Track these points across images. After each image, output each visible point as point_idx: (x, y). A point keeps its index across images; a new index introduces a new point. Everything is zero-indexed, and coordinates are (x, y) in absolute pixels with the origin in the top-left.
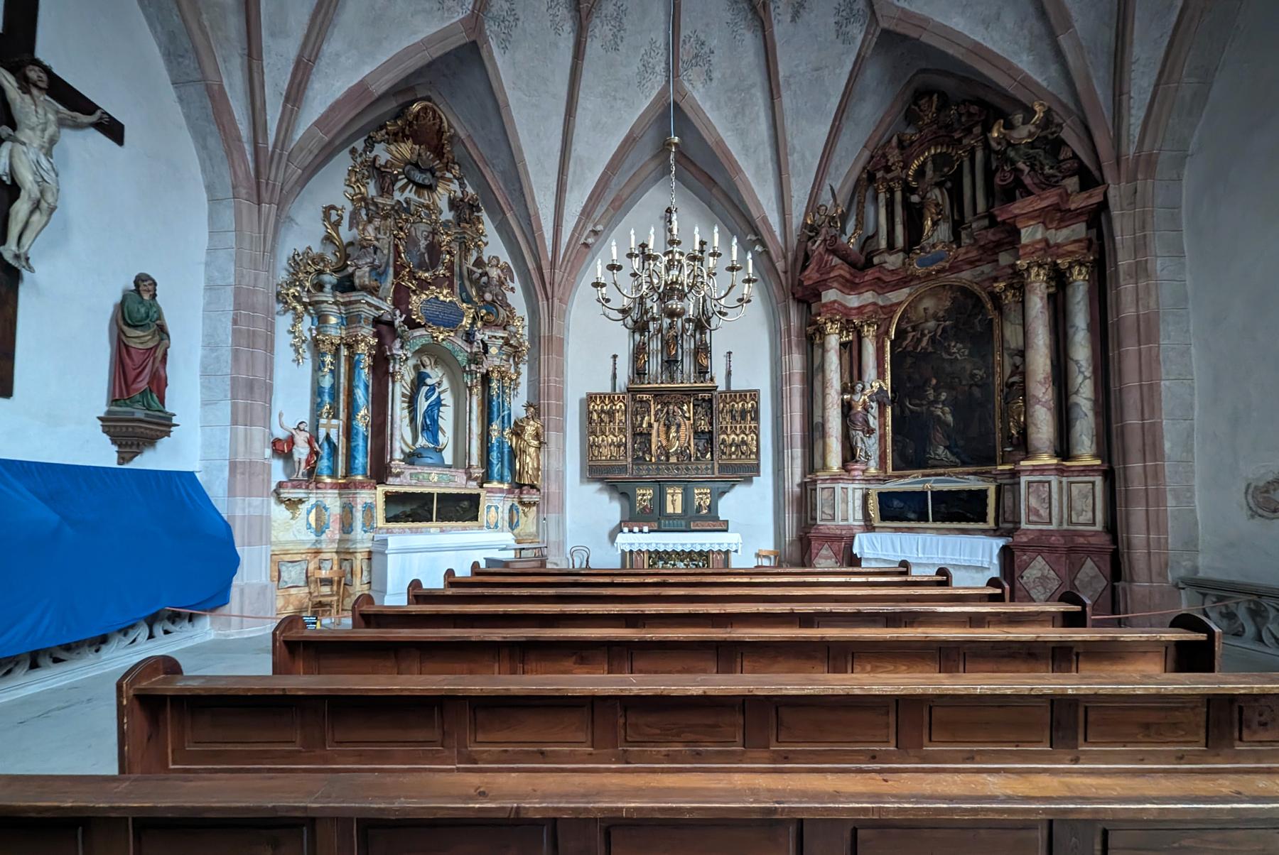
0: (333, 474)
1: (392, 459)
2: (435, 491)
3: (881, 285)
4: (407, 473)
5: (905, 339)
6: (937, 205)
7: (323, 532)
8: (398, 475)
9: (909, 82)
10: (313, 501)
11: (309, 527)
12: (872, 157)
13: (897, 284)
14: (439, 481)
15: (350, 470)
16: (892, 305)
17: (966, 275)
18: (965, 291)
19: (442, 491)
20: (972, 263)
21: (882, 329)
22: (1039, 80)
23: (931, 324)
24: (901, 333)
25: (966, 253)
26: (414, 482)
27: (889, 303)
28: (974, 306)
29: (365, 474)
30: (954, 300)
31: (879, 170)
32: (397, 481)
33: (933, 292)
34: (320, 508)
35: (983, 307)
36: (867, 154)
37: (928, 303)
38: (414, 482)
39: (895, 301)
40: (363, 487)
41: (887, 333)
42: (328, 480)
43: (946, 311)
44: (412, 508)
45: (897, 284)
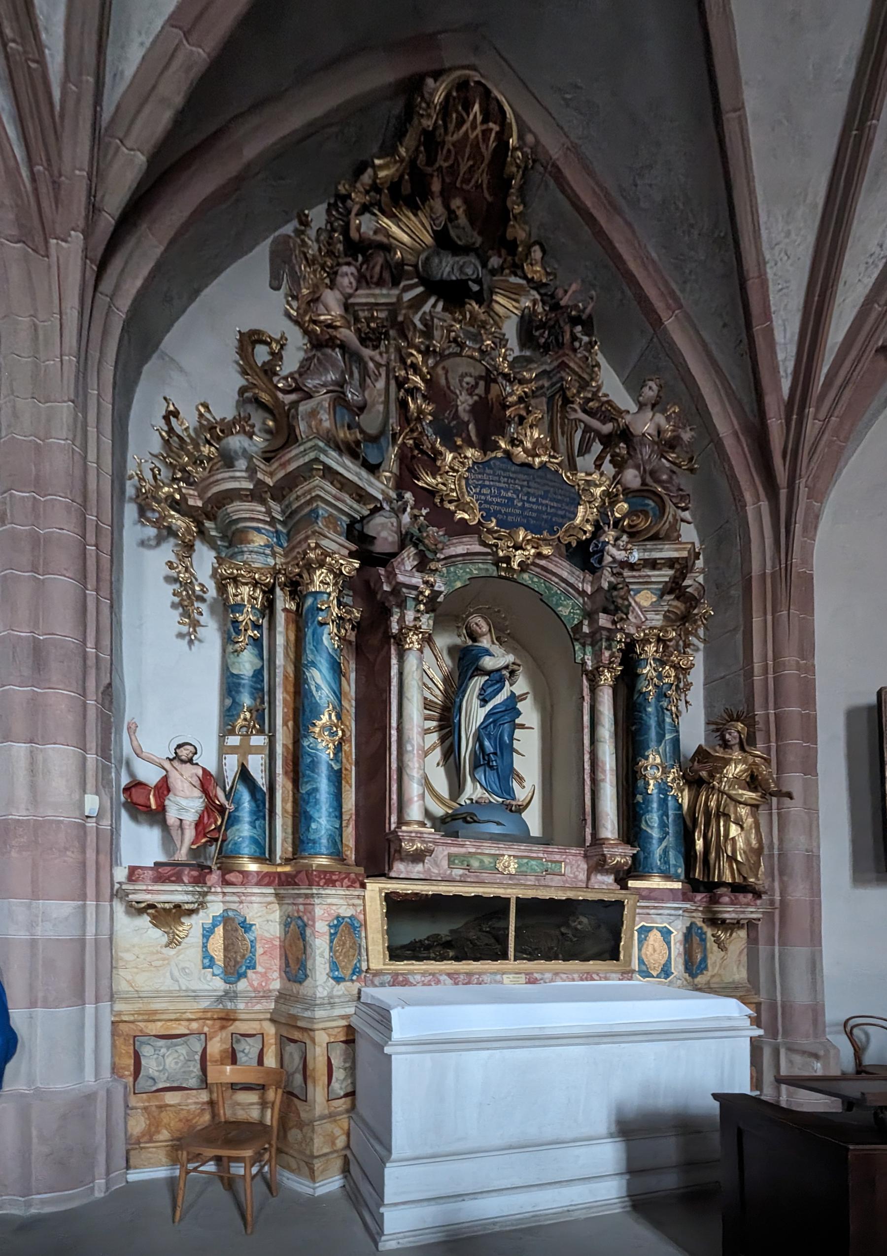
0: (264, 855)
1: (401, 822)
2: (512, 893)
4: (442, 853)
7: (242, 976)
8: (418, 857)
10: (215, 907)
11: (209, 962)
14: (520, 873)
15: (301, 842)
19: (530, 894)
26: (457, 872)
29: (337, 854)
32: (417, 870)
34: (234, 926)
38: (457, 872)
40: (331, 883)
42: (253, 867)
44: (458, 931)
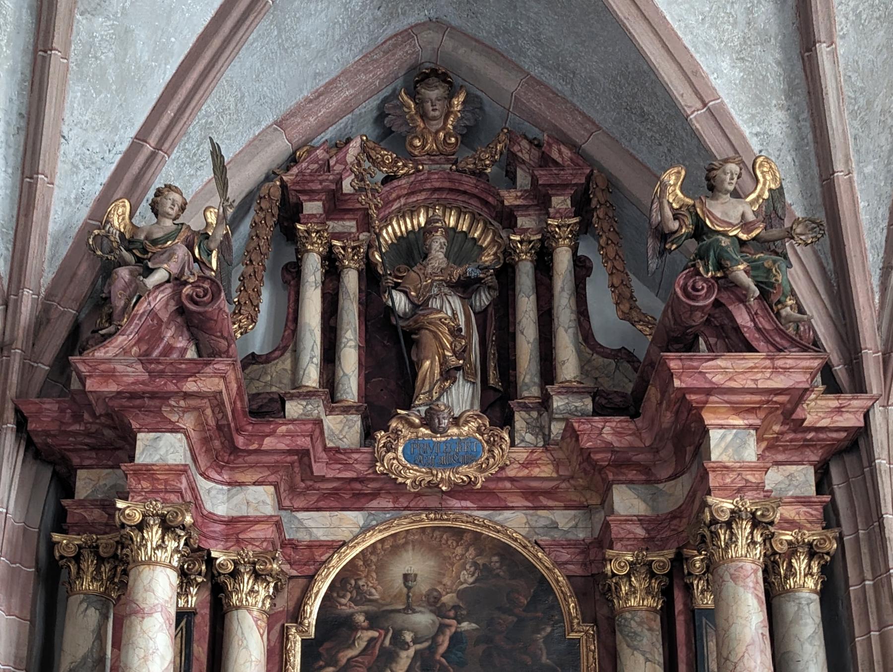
3: (302, 478)
5: (351, 646)
6: (455, 332)
9: (407, 35)
12: (293, 160)
13: (335, 494)
16: (313, 546)
17: (514, 523)
18: (508, 562)
20: (534, 496)
21: (282, 603)
22: (746, 131)
23: (423, 619)
24: (334, 626)
25: (526, 464)
27: (303, 537)
28: (534, 600)
30: (484, 572)
31: (312, 194)
33: (430, 540)
35: (555, 606)
36: (281, 146)
37: (415, 564)
39: (321, 535)
41: (297, 615)
43: (461, 594)
45: (335, 494)
